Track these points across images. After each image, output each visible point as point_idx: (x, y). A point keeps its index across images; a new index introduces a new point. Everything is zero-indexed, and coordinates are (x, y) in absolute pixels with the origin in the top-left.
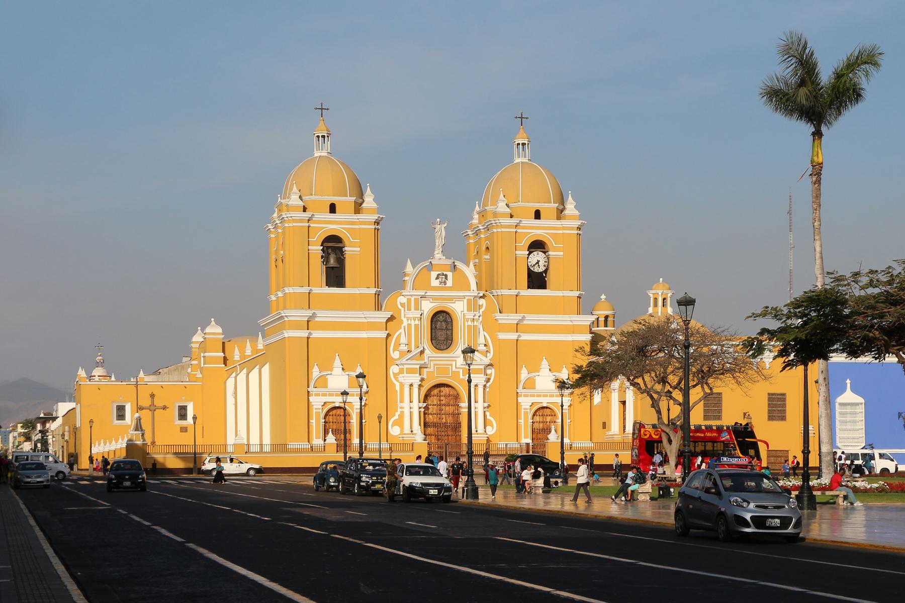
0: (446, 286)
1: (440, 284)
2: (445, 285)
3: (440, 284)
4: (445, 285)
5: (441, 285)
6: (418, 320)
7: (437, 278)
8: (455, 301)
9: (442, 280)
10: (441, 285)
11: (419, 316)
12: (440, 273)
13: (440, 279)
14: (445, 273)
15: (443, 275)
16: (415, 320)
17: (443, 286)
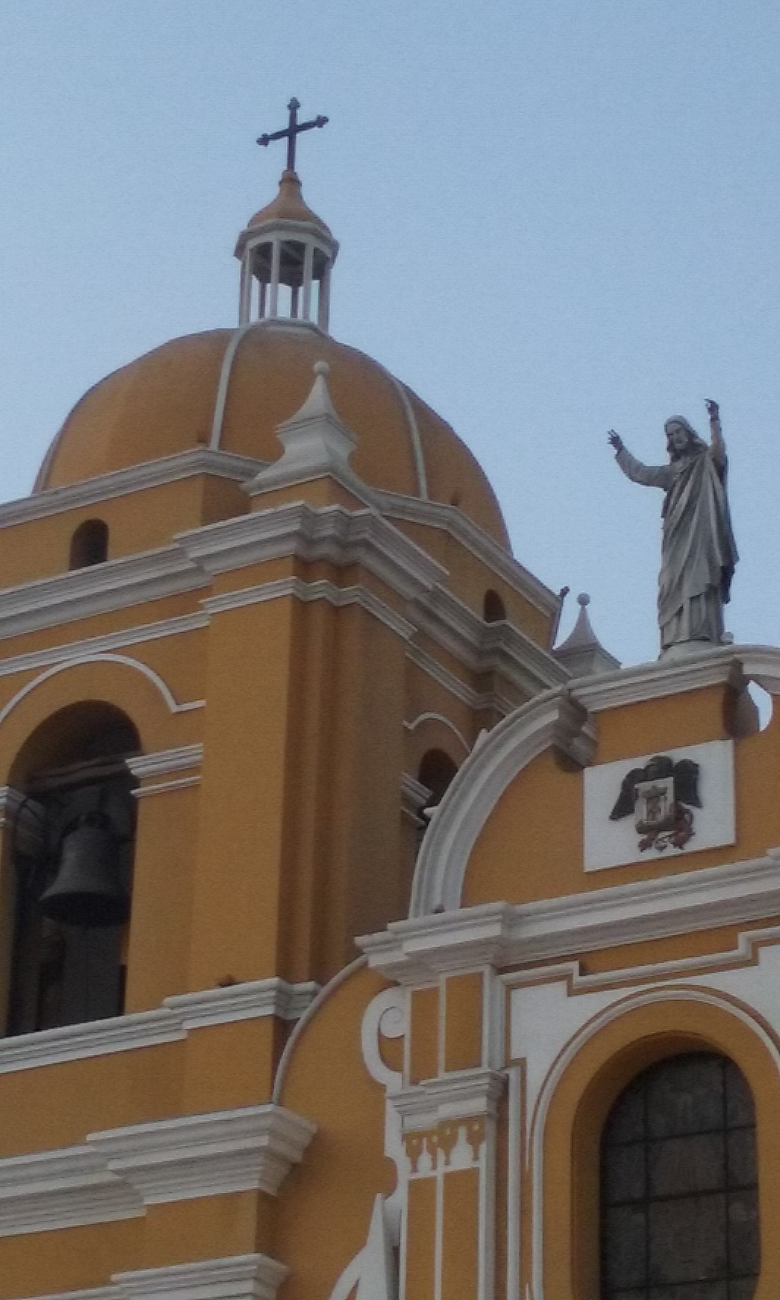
0: (690, 847)
1: (644, 846)
2: (679, 844)
3: (644, 846)
4: (679, 844)
5: (652, 854)
6: (474, 1140)
7: (623, 809)
8: (756, 945)
9: (652, 813)
10: (652, 854)
11: (479, 1105)
12: (640, 763)
13: (641, 810)
14: (678, 755)
15: (662, 768)
16: (448, 1144)
17: (671, 851)
